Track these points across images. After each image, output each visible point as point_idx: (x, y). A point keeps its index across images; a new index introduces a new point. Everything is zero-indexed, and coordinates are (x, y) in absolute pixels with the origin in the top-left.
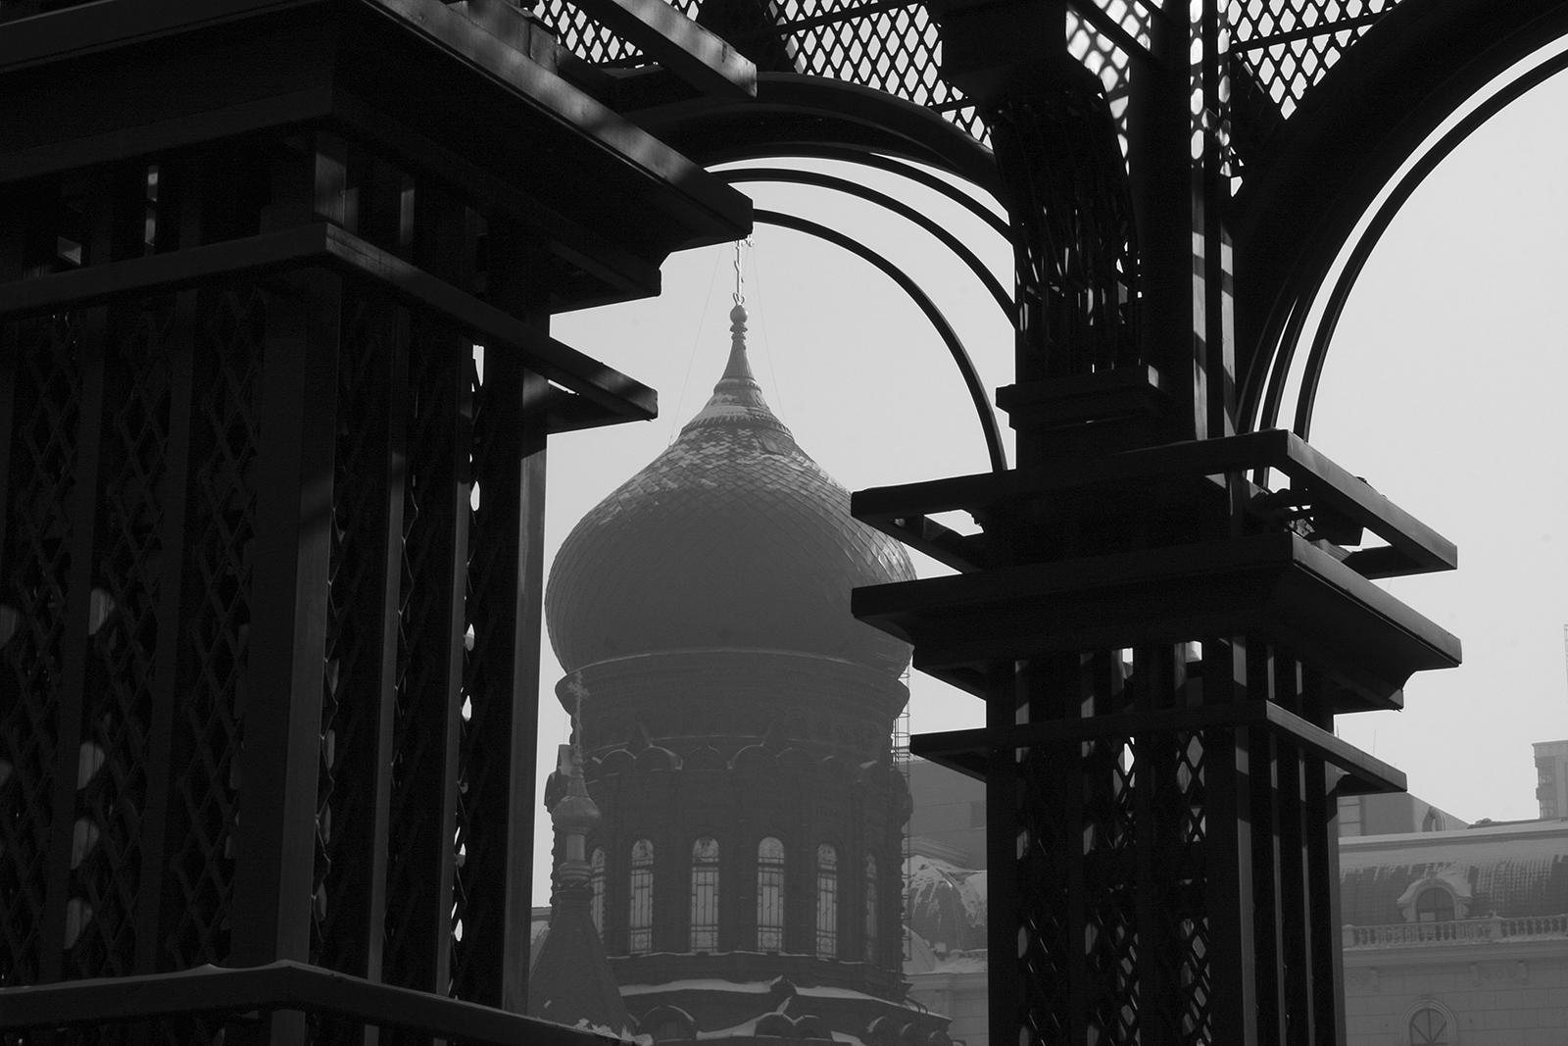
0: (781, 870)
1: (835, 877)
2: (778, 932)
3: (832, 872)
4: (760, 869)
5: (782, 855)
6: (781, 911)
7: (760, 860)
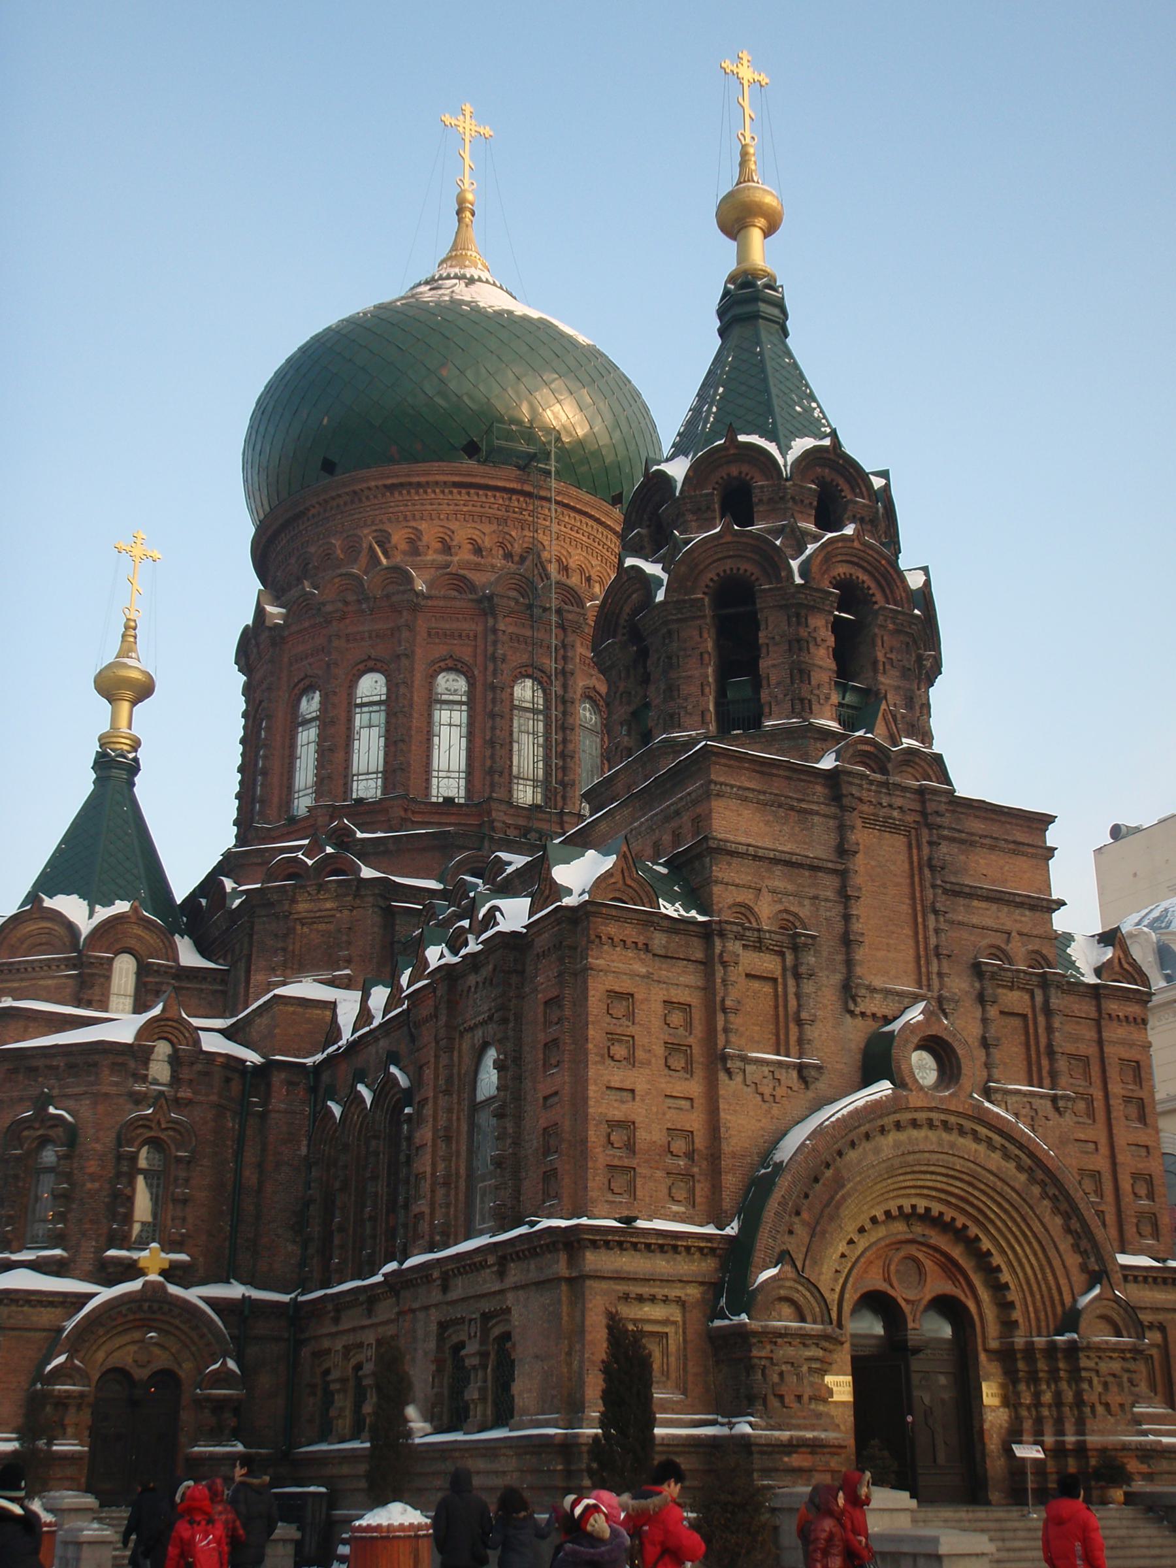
0: (383, 708)
1: (464, 708)
2: (377, 778)
3: (460, 703)
4: (358, 710)
5: (384, 690)
6: (382, 754)
7: (359, 701)
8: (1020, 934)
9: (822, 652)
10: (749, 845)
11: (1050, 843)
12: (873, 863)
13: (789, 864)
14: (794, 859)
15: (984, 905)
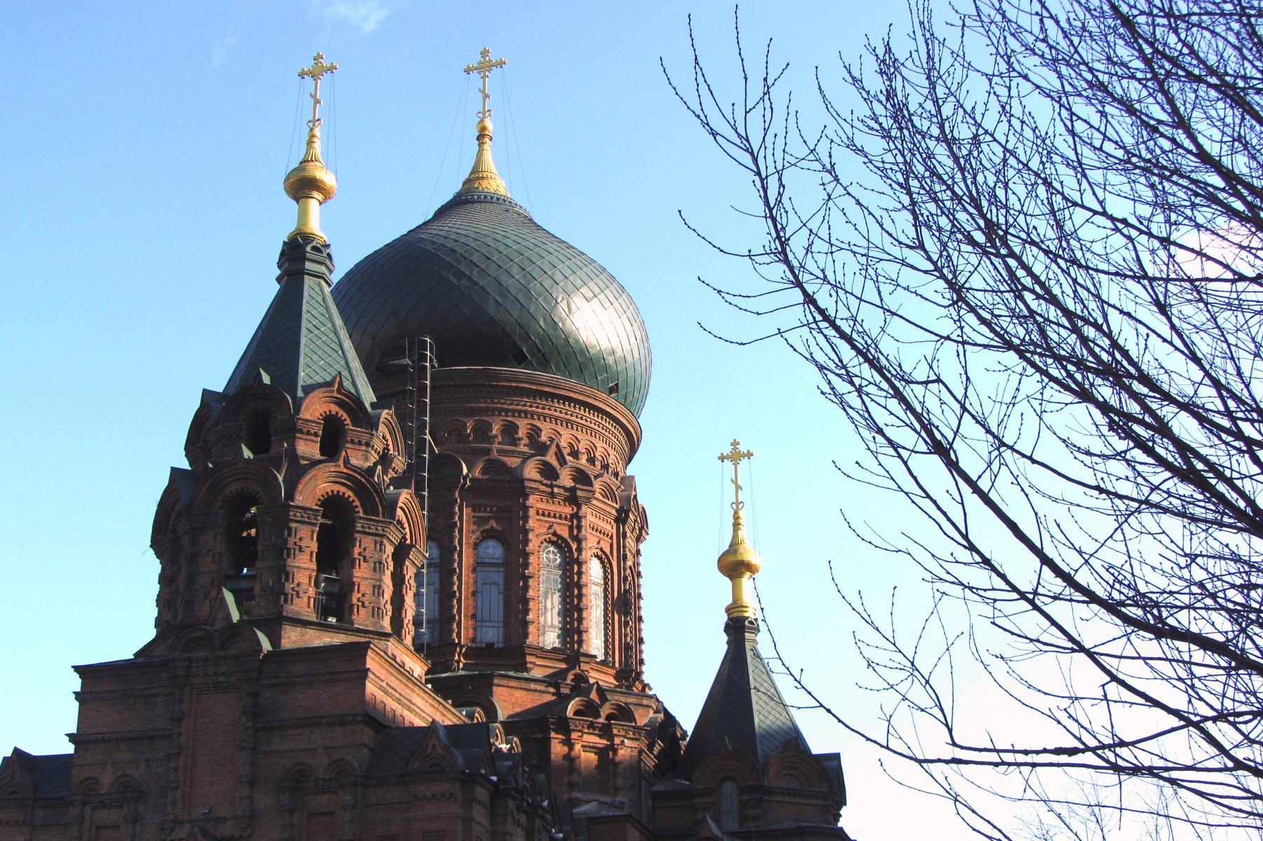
8: (325, 748)
9: (208, 559)
10: (97, 734)
11: (367, 666)
12: (207, 720)
13: (133, 740)
14: (132, 735)
15: (298, 731)
